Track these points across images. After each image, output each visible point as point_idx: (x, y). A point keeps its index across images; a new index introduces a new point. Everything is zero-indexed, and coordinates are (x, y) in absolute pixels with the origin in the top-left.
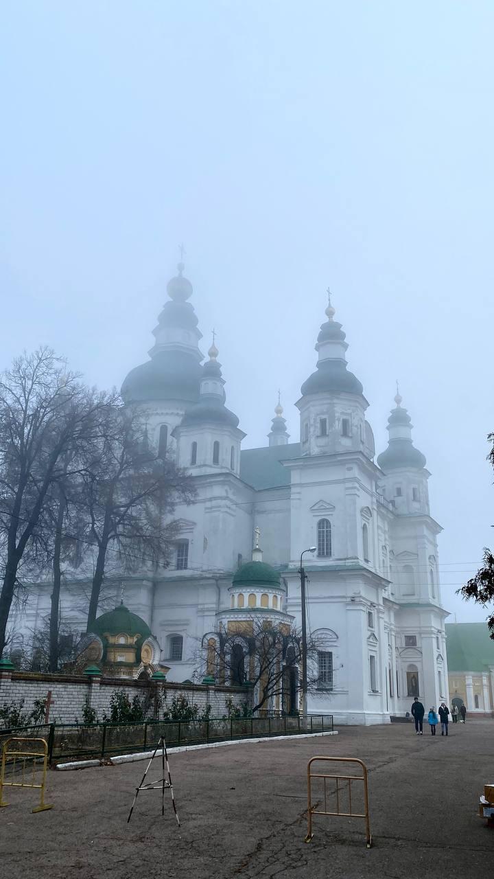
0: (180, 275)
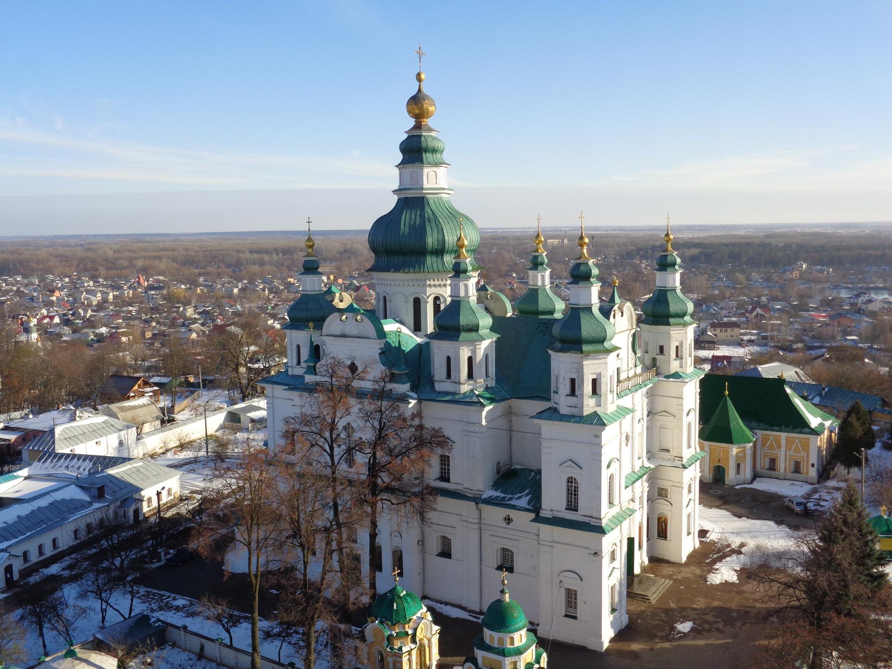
0: (419, 91)
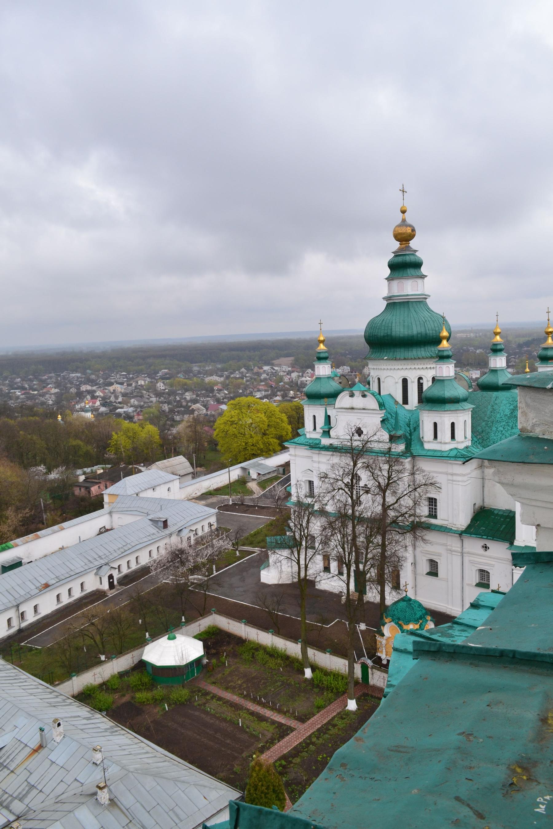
0: (404, 220)
